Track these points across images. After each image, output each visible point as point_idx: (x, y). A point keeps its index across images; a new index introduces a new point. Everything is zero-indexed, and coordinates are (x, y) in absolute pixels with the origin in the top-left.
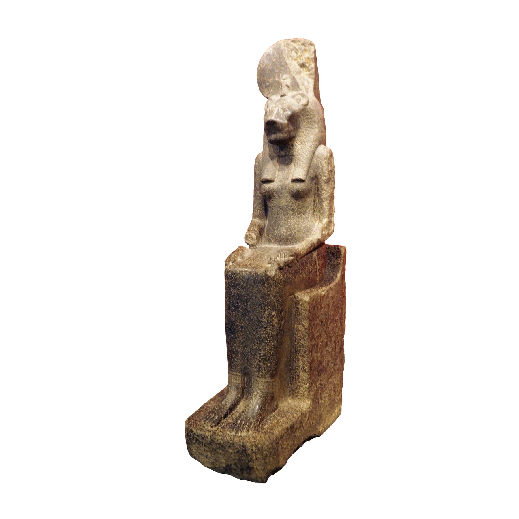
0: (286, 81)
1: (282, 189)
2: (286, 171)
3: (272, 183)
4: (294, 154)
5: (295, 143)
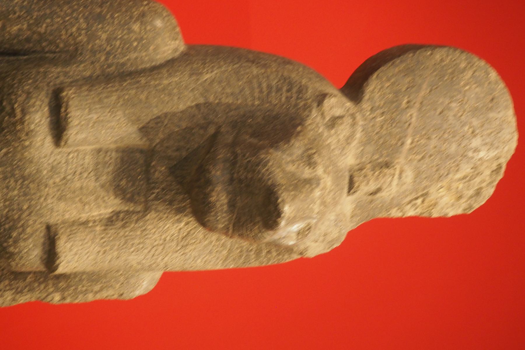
0: (395, 182)
1: (24, 178)
2: (92, 184)
3: (49, 140)
4: (152, 215)
5: (186, 219)
